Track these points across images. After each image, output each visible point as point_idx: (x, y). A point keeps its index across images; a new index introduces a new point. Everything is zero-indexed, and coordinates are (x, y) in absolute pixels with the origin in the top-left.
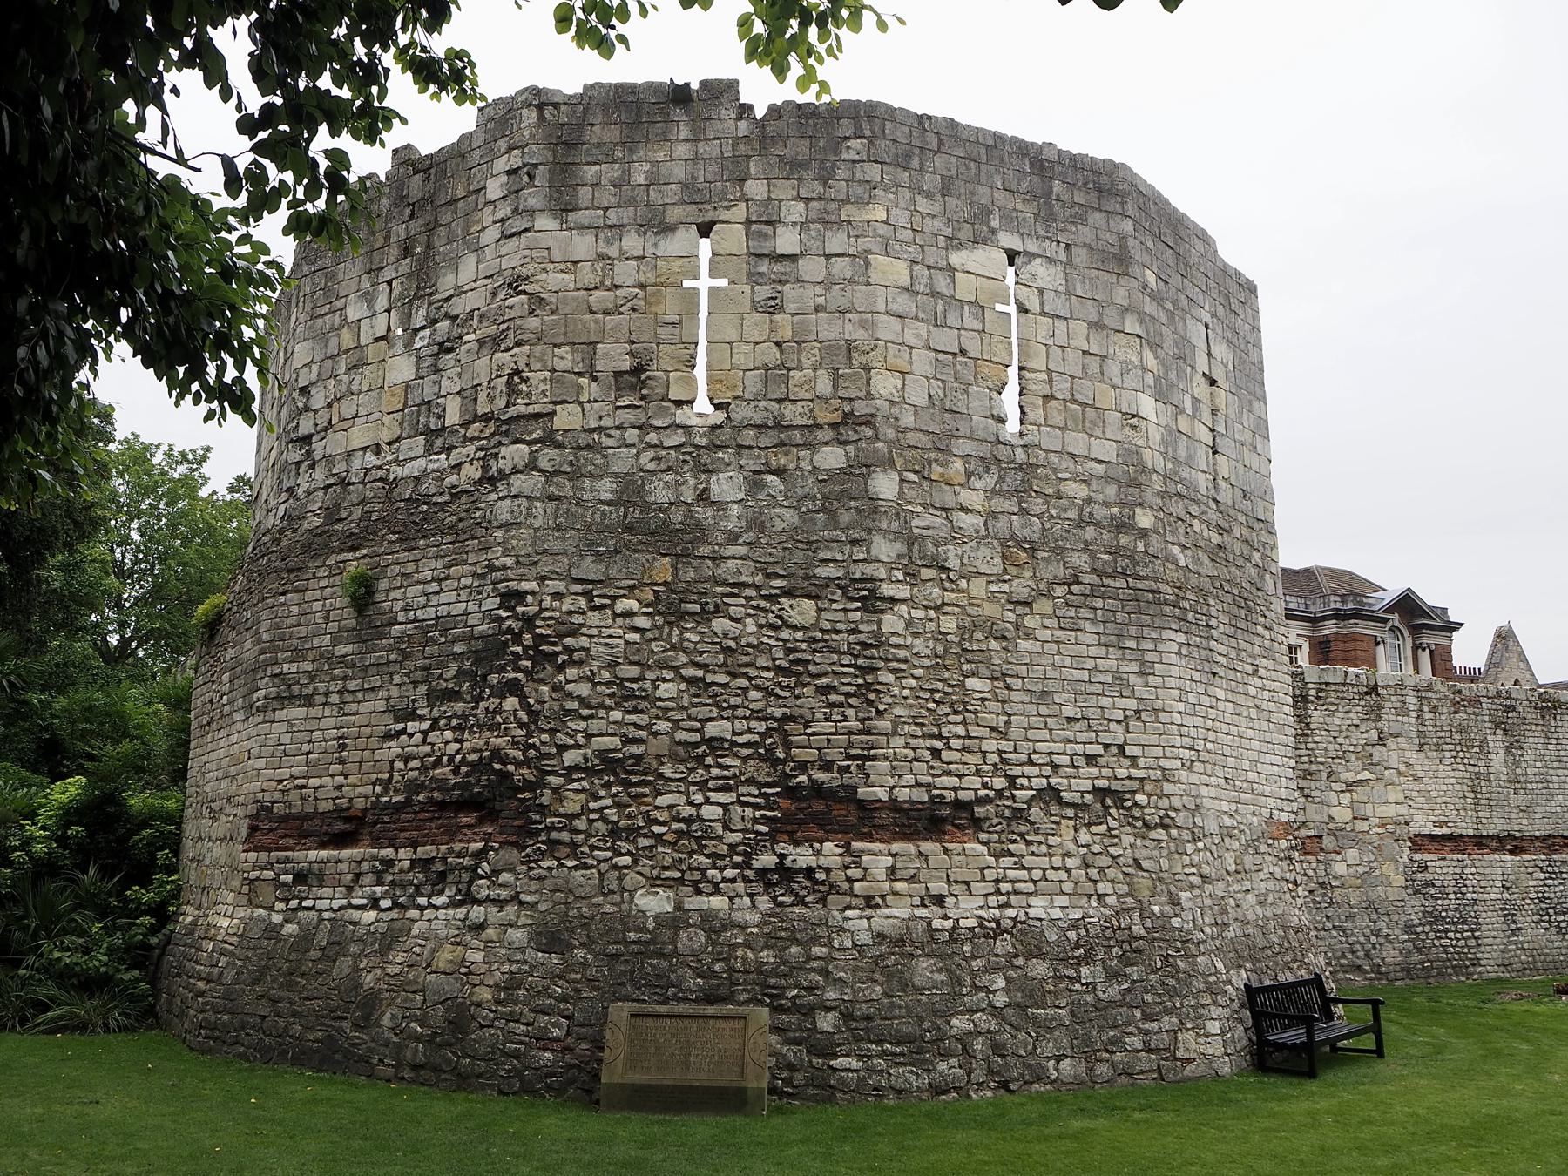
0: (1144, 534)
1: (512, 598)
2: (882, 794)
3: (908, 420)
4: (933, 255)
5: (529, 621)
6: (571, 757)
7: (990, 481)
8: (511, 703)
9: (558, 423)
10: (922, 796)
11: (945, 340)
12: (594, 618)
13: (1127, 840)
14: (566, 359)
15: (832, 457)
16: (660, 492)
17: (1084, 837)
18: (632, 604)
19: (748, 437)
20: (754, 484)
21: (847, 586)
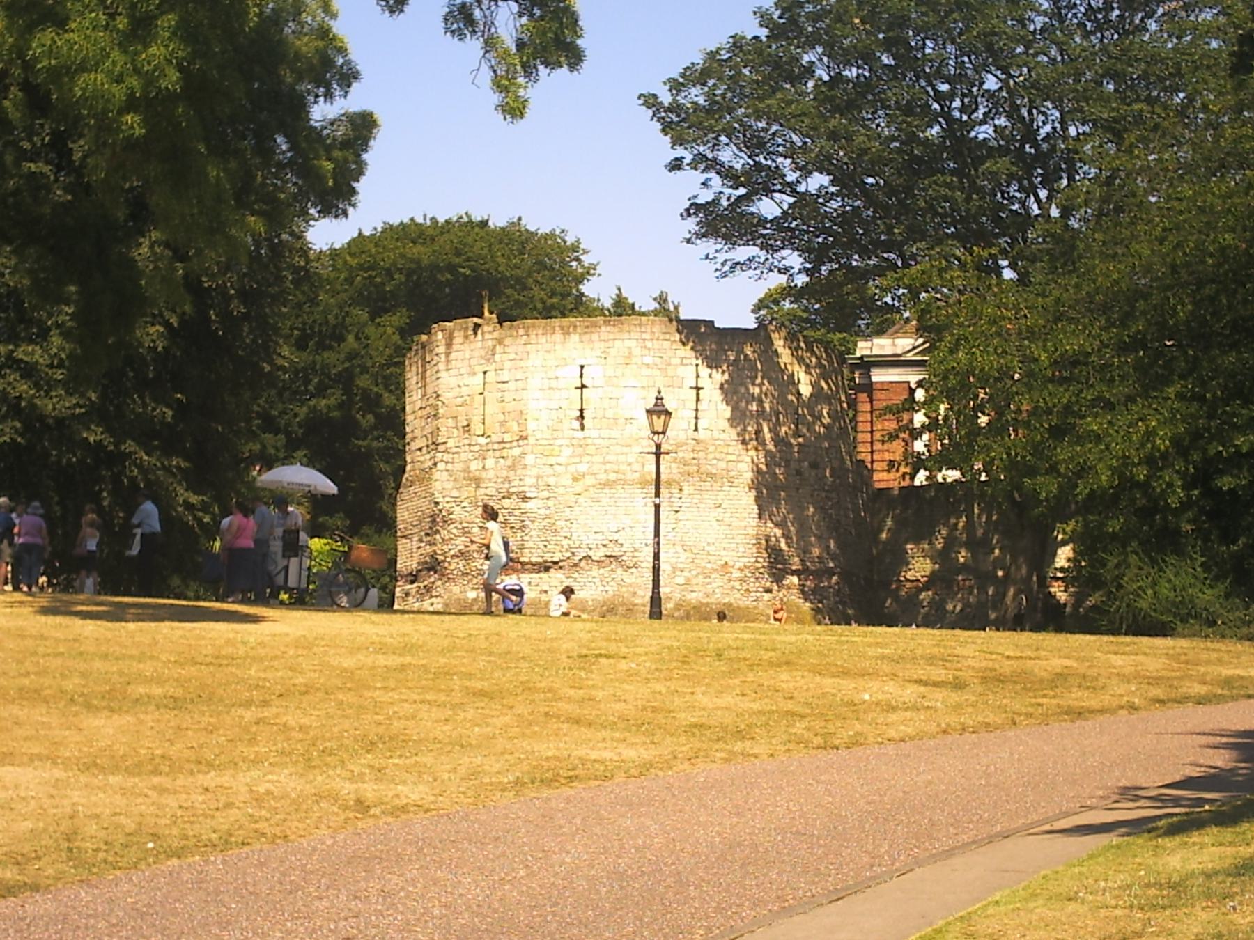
0: (630, 464)
1: (437, 503)
2: (526, 560)
3: (539, 435)
4: (551, 375)
5: (440, 511)
6: (452, 552)
7: (567, 452)
8: (438, 536)
9: (448, 445)
10: (540, 560)
11: (555, 405)
12: (457, 509)
13: (620, 571)
14: (451, 422)
15: (516, 452)
16: (474, 466)
17: (602, 571)
18: (465, 504)
19: (496, 446)
20: (497, 463)
21: (518, 494)
